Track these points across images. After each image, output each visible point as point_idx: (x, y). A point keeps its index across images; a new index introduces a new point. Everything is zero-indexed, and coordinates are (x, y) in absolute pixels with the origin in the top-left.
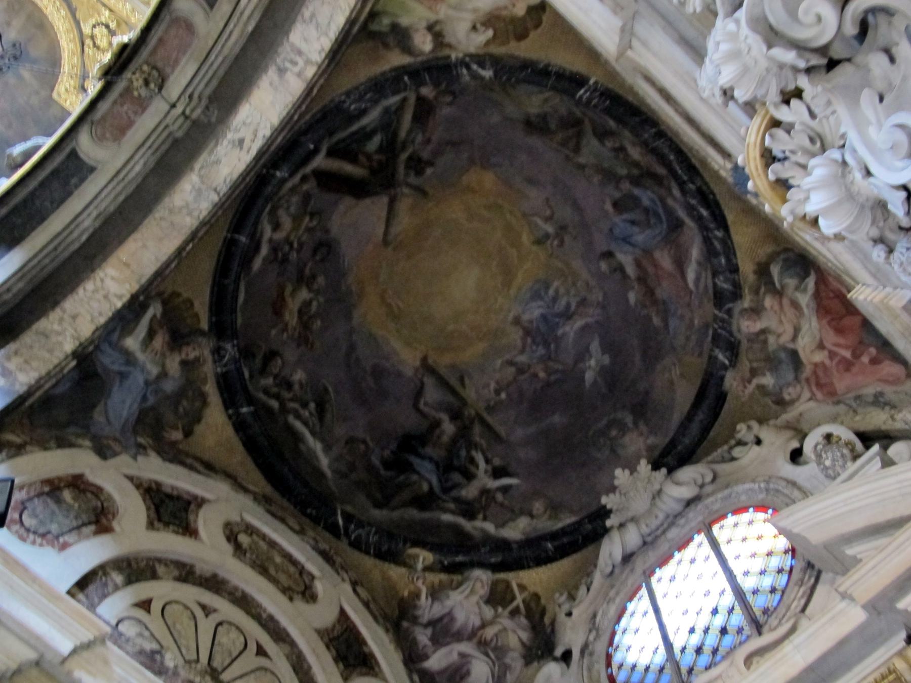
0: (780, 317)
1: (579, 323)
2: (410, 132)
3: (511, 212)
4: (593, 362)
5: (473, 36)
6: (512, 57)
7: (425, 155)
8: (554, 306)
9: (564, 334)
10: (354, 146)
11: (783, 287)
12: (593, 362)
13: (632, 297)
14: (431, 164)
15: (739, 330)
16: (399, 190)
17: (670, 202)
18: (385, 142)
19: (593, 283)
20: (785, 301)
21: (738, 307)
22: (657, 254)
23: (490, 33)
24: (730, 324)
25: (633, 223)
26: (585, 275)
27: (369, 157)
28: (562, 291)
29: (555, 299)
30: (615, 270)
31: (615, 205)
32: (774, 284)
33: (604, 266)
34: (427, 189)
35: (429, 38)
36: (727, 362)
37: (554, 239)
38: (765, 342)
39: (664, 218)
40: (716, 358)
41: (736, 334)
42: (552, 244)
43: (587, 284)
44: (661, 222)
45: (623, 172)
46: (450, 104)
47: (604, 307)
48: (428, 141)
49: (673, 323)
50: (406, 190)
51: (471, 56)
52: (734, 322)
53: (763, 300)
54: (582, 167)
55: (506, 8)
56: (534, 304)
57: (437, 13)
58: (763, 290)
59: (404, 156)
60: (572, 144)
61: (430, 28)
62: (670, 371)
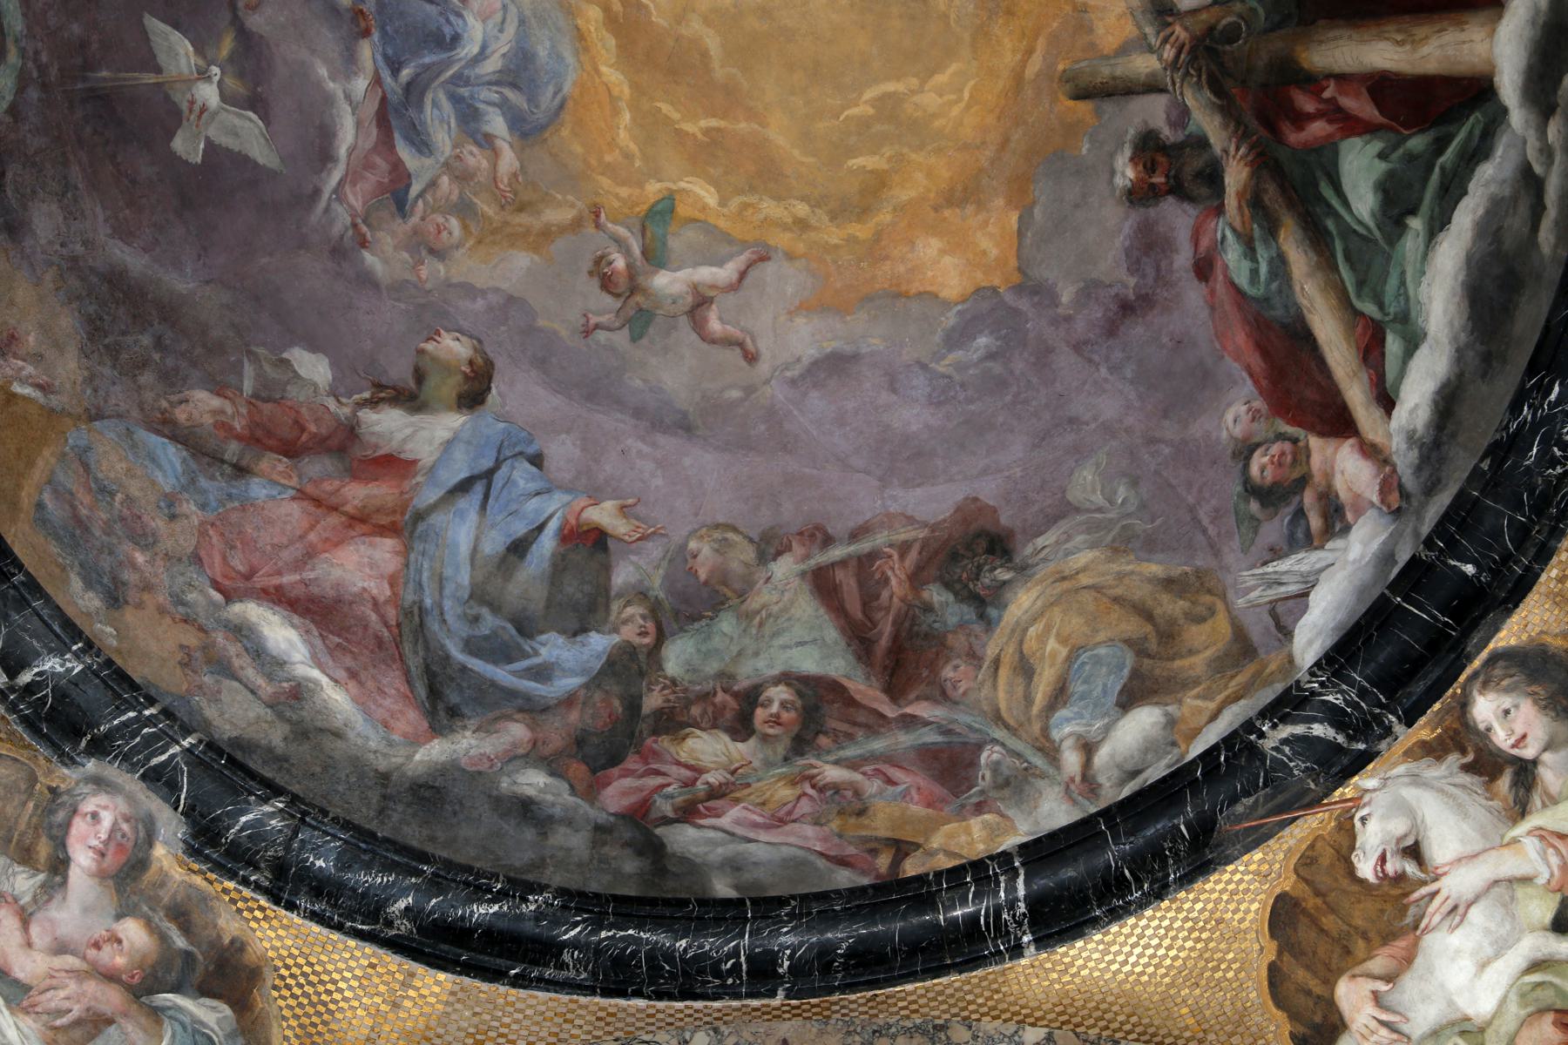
0: (73, 953)
1: (348, 134)
2: (1280, 265)
3: (802, 225)
4: (208, 93)
5: (1399, 826)
6: (1257, 839)
7: (1177, 217)
8: (456, 100)
9: (350, 59)
10: (1417, 143)
11: (156, 1013)
12: (208, 93)
13: (314, 368)
14: (1139, 195)
15: (99, 783)
16: (1169, 53)
17: (517, 732)
18: (1327, 192)
19: (431, 270)
20: (110, 998)
21: (171, 828)
22: (384, 551)
23: (1366, 868)
24: (126, 758)
25: (519, 548)
26: (468, 267)
27: (1353, 126)
28: (475, 158)
29: (468, 116)
30: (420, 376)
31: (596, 541)
32: (176, 989)
33: (454, 348)
34: (1084, 108)
35: (1502, 738)
36: (26, 677)
37: (629, 266)
38: (25, 856)
39: (476, 664)
40: (61, 651)
41: (91, 765)
42: (619, 242)
43: (437, 253)
44: (471, 647)
45: (677, 657)
46: (1245, 450)
47: (338, 252)
48: (1204, 268)
49: (172, 455)
50: (1144, 65)
51: (1360, 762)
52: (131, 782)
53: (149, 925)
54: (769, 547)
55: (1390, 978)
56: (503, 45)
57: (1542, 834)
58: (180, 942)
59: (1235, 176)
60: (847, 581)
61: (1525, 772)
62: (37, 358)
